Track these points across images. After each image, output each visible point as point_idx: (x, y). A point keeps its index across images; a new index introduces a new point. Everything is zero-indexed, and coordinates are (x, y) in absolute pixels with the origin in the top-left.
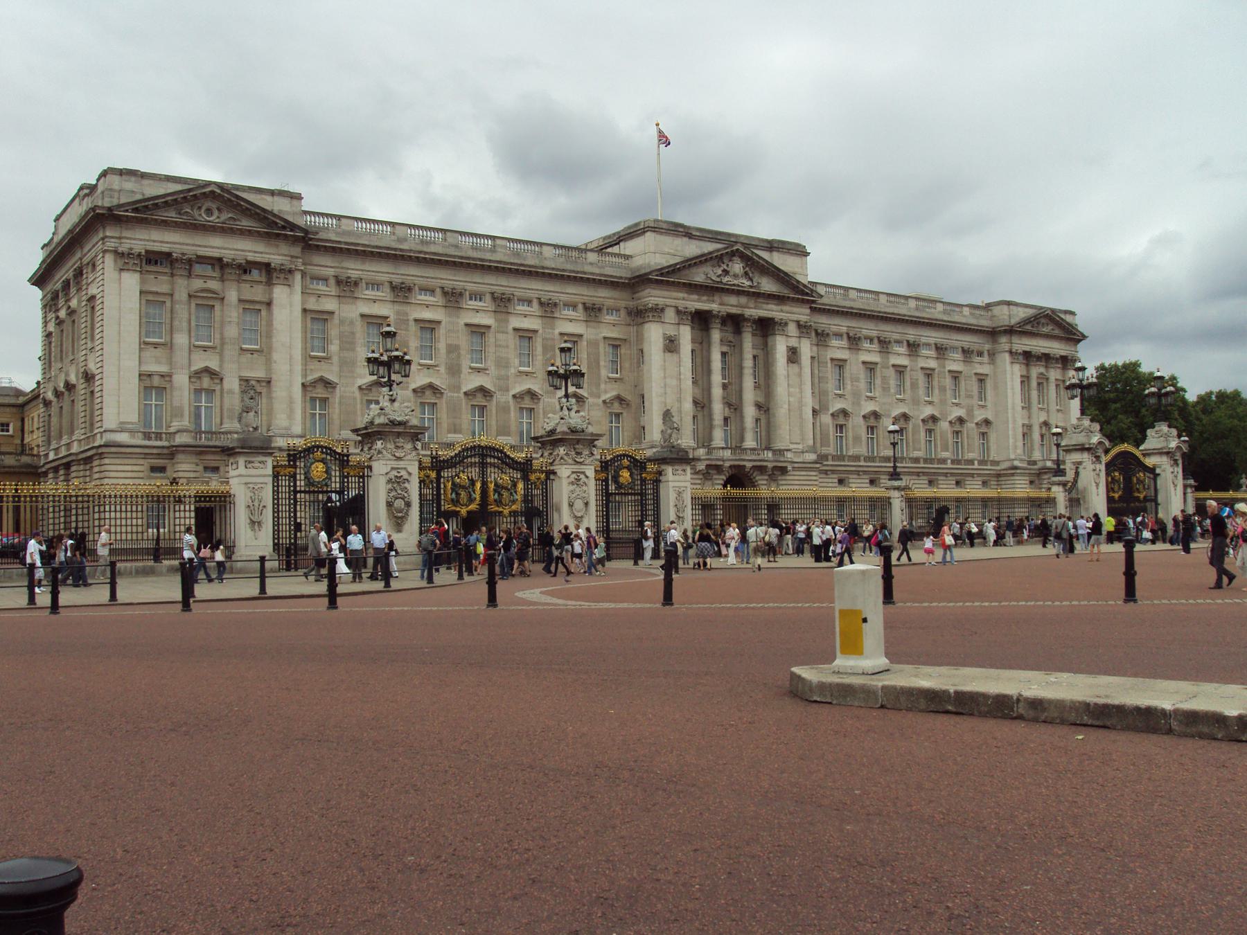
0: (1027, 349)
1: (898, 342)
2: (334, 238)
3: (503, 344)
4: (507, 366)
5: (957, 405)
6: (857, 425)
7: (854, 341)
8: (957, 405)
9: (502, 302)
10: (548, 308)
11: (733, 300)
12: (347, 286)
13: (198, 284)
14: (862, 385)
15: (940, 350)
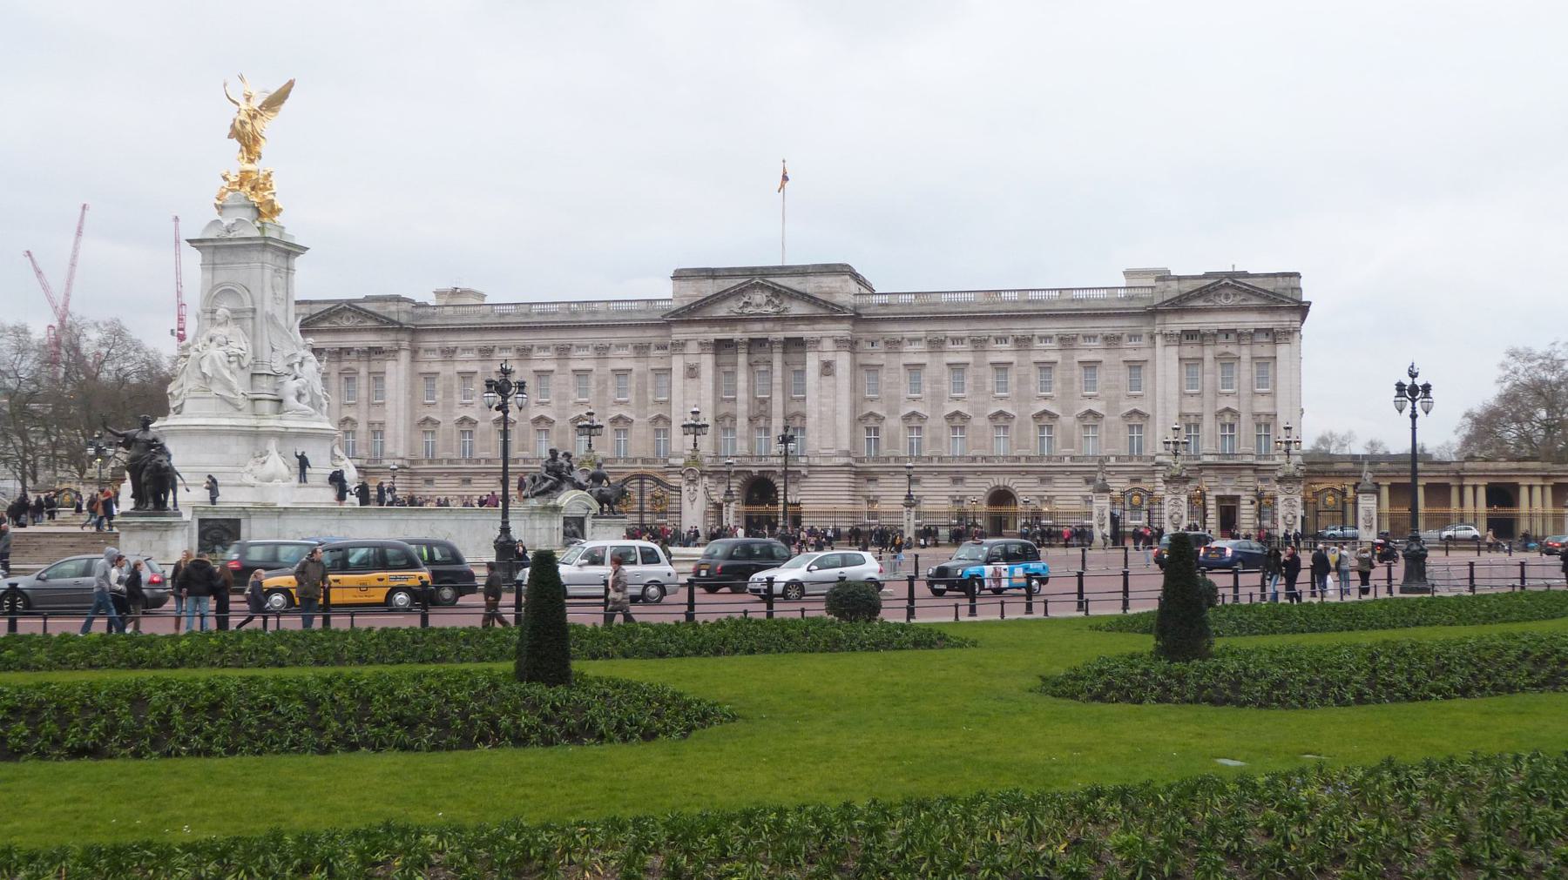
0: (1195, 327)
1: (997, 340)
2: (437, 321)
3: (562, 381)
4: (566, 399)
5: (1090, 397)
6: (936, 423)
7: (936, 345)
8: (1090, 397)
9: (563, 351)
10: (602, 351)
11: (758, 326)
12: (448, 353)
13: (346, 365)
14: (946, 387)
15: (1067, 342)
